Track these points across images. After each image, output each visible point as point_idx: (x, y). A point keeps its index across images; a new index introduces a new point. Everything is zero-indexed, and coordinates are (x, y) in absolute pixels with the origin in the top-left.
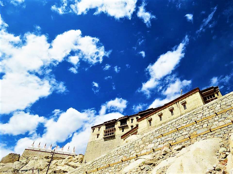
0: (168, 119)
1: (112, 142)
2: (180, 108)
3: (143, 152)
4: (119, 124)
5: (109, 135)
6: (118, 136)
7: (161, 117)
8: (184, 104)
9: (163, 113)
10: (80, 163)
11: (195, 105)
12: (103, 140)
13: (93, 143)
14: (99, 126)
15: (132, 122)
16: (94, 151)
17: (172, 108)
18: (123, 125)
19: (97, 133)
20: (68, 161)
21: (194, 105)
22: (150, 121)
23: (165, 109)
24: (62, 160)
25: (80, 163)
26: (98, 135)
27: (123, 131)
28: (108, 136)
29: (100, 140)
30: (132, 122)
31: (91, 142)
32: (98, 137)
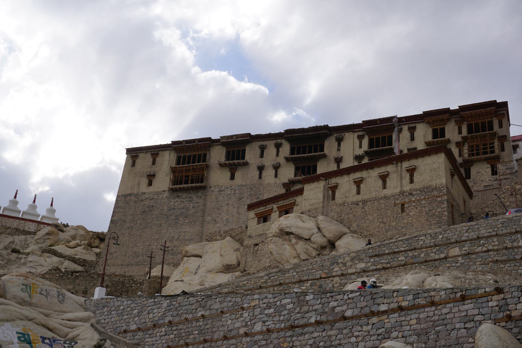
0: (374, 195)
1: (197, 205)
2: (401, 178)
3: (350, 271)
4: (217, 155)
5: (190, 185)
6: (217, 189)
7: (358, 187)
8: (412, 171)
9: (366, 178)
10: (84, 249)
11: (431, 180)
12: (166, 194)
13: (133, 198)
14: (155, 151)
15: (262, 156)
16: (139, 222)
17: (386, 173)
18: (236, 161)
19: (149, 170)
20: (48, 243)
21: (429, 179)
22: (334, 189)
23: (371, 171)
24: (23, 237)
25: (84, 249)
26: (151, 178)
27: (232, 178)
28: (185, 185)
29: (158, 193)
30: (262, 156)
31: (128, 198)
32: (150, 184)
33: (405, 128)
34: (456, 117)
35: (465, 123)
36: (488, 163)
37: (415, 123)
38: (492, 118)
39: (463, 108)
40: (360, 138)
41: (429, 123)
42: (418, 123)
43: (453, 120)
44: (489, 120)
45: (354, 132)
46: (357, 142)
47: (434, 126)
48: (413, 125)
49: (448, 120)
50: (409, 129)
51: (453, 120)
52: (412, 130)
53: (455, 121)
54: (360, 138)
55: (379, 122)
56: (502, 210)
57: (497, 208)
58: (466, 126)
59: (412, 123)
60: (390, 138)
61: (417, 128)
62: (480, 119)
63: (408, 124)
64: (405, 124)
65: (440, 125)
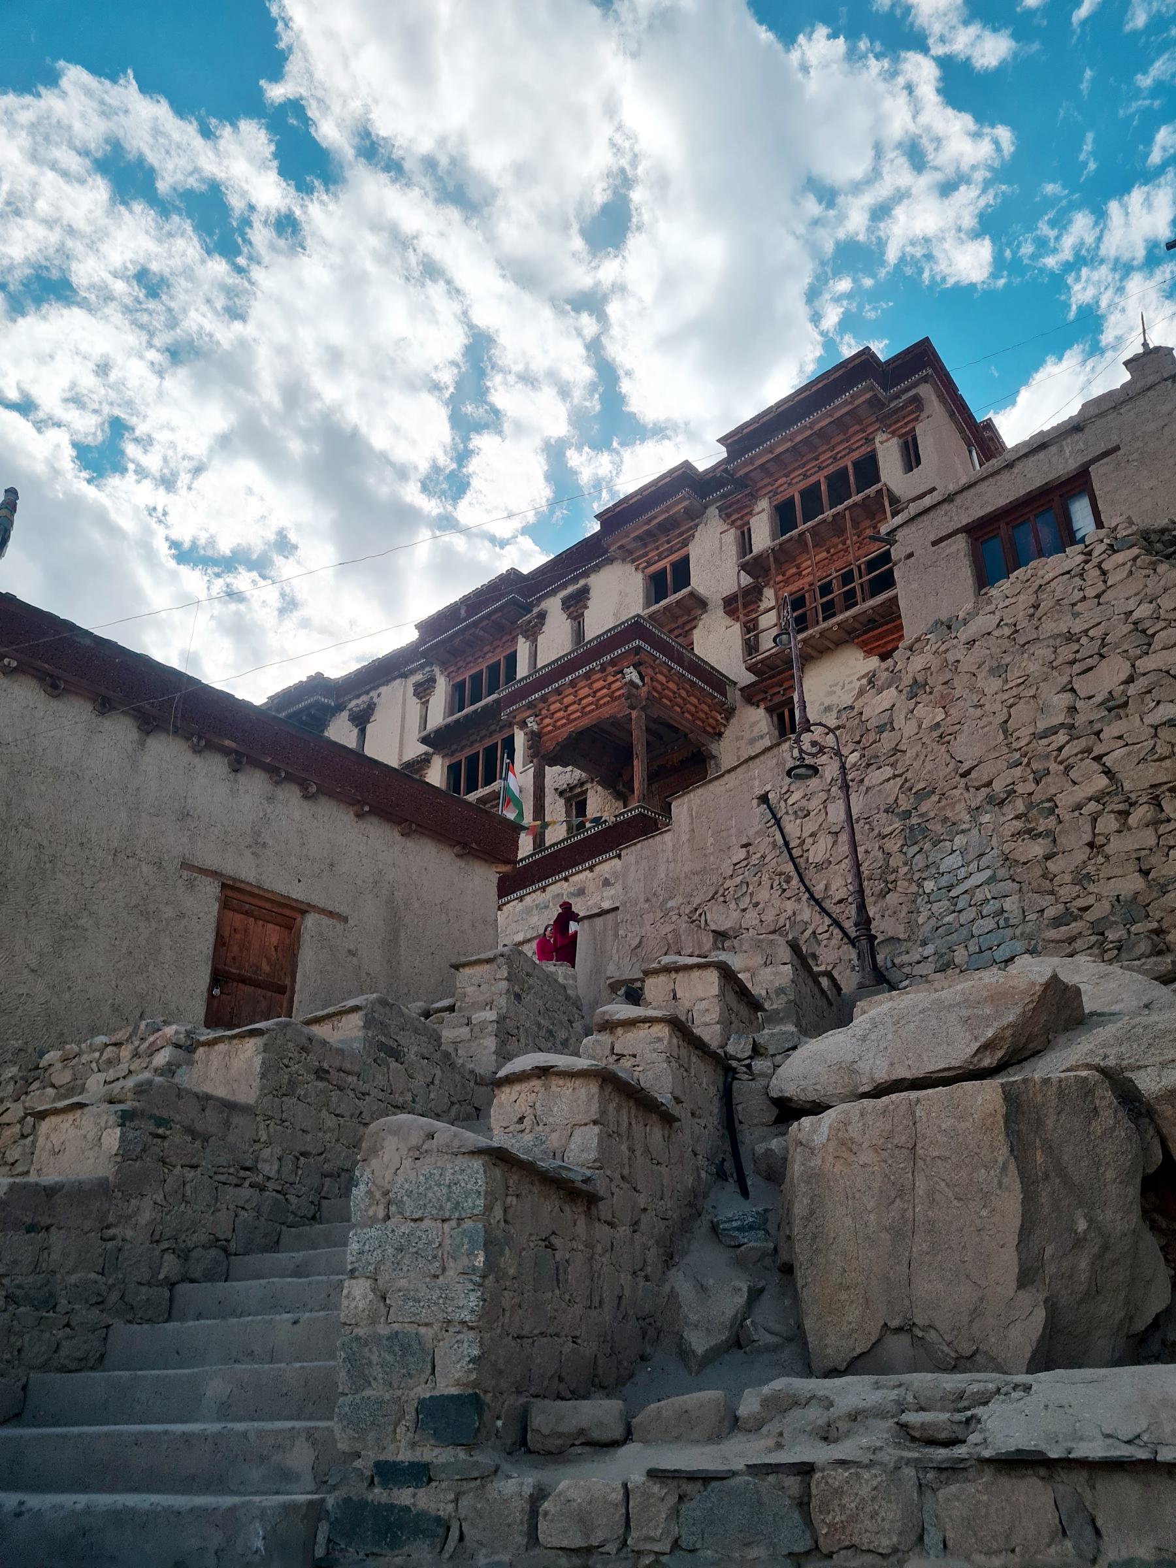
33: (553, 605)
34: (724, 496)
35: (763, 504)
36: (869, 653)
37: (586, 575)
38: (869, 440)
39: (740, 442)
40: (423, 691)
41: (627, 555)
42: (597, 568)
43: (713, 511)
44: (856, 455)
45: (405, 676)
46: (414, 705)
47: (649, 564)
48: (582, 582)
49: (695, 516)
50: (566, 604)
51: (713, 511)
52: (576, 605)
53: (720, 509)
54: (423, 691)
55: (463, 612)
56: (790, 906)
57: (763, 895)
58: (765, 517)
59: (575, 580)
60: (512, 659)
61: (592, 593)
62: (820, 469)
63: (564, 586)
64: (554, 593)
65: (671, 551)
